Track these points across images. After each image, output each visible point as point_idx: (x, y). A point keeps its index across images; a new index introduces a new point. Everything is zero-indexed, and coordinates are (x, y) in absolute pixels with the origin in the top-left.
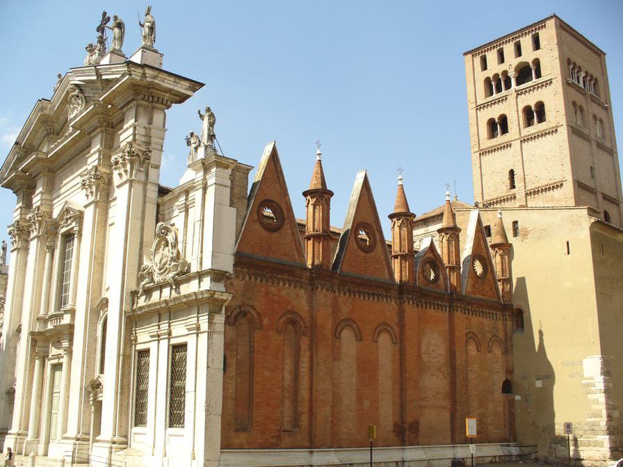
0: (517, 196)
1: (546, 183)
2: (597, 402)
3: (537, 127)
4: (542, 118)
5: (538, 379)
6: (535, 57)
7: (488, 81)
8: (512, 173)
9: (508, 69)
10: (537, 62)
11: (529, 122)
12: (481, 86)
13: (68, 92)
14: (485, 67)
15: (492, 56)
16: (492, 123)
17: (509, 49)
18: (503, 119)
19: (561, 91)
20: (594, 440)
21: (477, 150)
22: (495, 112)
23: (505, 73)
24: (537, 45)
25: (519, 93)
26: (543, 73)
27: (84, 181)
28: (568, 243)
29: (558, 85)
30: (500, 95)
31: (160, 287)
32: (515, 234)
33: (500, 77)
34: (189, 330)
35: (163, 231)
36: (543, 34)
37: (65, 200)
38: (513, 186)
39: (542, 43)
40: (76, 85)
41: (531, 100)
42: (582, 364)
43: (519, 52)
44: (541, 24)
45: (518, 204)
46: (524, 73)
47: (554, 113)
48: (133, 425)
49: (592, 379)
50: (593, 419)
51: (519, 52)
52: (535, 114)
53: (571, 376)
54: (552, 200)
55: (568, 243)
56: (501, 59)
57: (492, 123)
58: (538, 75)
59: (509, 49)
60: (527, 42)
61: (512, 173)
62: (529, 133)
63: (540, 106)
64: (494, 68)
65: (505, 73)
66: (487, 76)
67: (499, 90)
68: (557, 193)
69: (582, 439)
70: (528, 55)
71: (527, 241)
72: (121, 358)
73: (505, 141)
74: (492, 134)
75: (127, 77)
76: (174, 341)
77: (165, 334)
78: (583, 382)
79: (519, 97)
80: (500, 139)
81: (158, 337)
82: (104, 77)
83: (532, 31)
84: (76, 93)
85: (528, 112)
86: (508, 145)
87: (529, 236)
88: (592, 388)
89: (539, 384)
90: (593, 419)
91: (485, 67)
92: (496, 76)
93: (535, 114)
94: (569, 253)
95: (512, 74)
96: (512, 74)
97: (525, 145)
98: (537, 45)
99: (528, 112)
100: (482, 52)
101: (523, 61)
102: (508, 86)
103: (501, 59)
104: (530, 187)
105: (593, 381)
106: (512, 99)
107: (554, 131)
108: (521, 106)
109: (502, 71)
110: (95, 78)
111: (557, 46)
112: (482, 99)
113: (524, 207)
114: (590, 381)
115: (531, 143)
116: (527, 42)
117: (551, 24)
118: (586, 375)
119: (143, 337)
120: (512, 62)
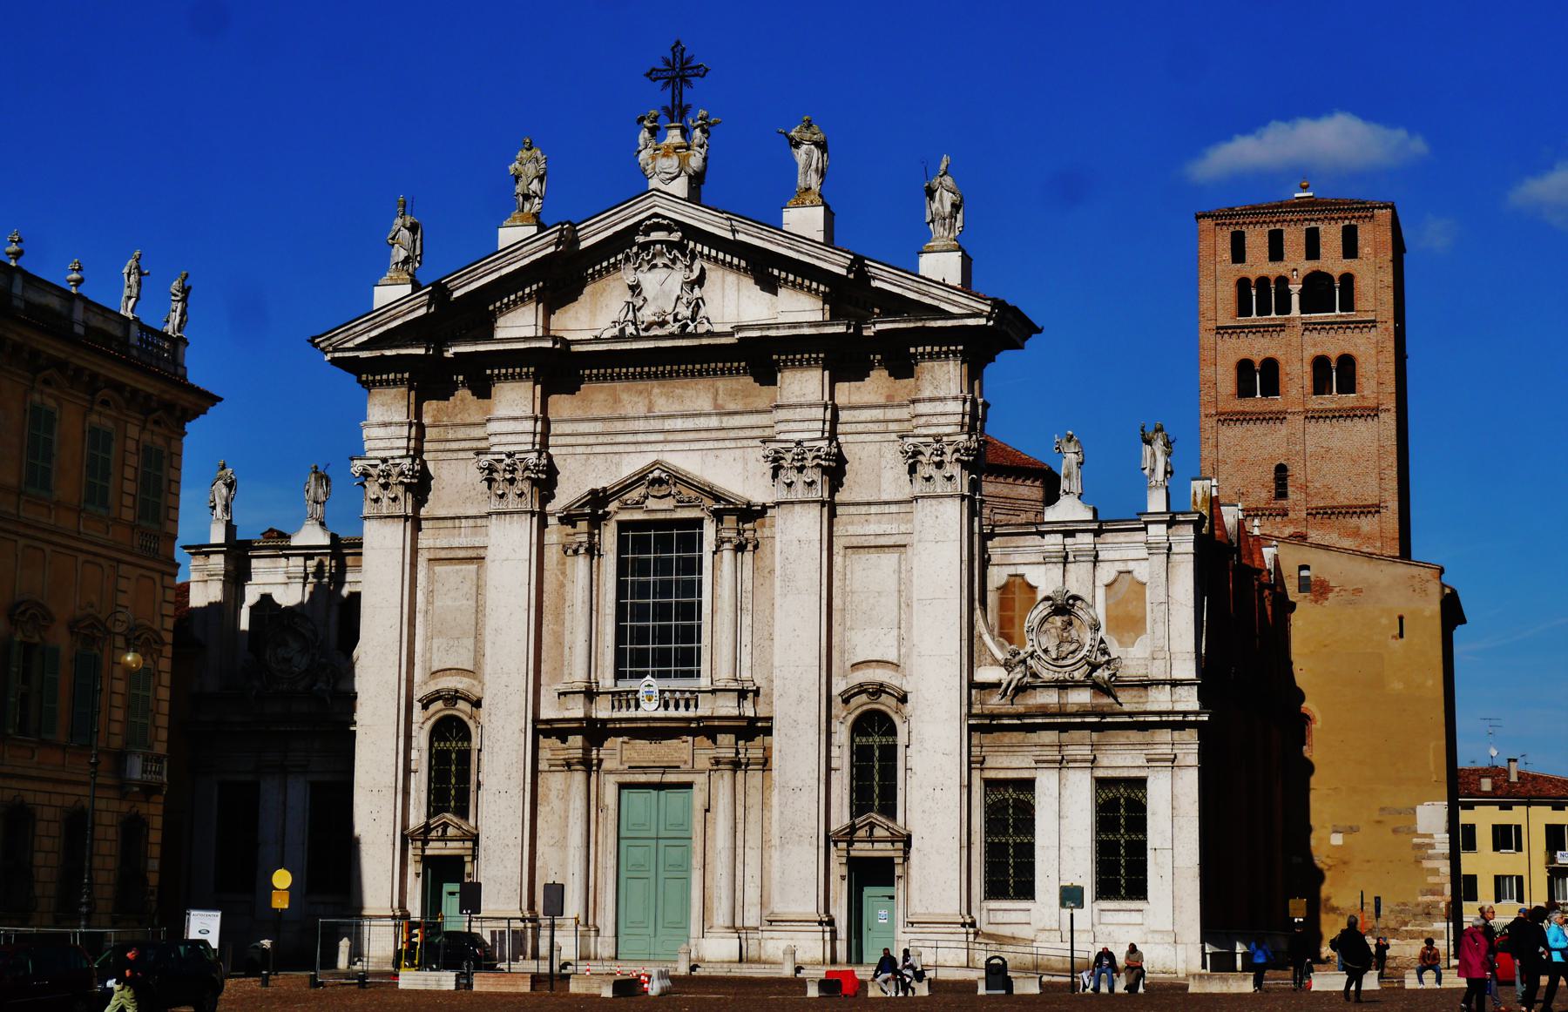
0: (1291, 514)
1: (1346, 503)
2: (1436, 872)
3: (1333, 400)
4: (1348, 385)
5: (1336, 832)
6: (1346, 270)
7: (1243, 285)
8: (1281, 471)
9: (1290, 277)
10: (1348, 279)
11: (1320, 387)
12: (1228, 293)
13: (634, 229)
14: (1238, 254)
15: (1257, 240)
16: (1244, 367)
17: (1294, 238)
18: (1271, 366)
19: (1393, 351)
20: (1429, 929)
21: (1214, 412)
22: (1257, 348)
23: (1283, 281)
24: (1350, 248)
25: (1308, 327)
26: (1359, 305)
27: (776, 452)
28: (1401, 618)
29: (1384, 335)
30: (1264, 320)
31: (1062, 686)
32: (1305, 584)
33: (1273, 286)
34: (1148, 761)
35: (1071, 602)
36: (1365, 234)
37: (649, 459)
38: (1281, 493)
39: (1365, 249)
40: (682, 226)
41: (1333, 346)
42: (1415, 812)
43: (1313, 251)
44: (1365, 209)
45: (1288, 531)
46: (1319, 292)
47: (1373, 383)
48: (983, 899)
49: (1431, 836)
50: (1429, 898)
51: (1313, 251)
52: (1334, 374)
53: (1395, 831)
54: (1356, 533)
55: (1401, 618)
56: (1276, 253)
57: (1244, 367)
58: (1348, 305)
59: (1294, 238)
60: (1331, 235)
61: (1281, 471)
62: (1321, 407)
63: (1347, 362)
64: (1258, 264)
65: (1283, 281)
66: (1243, 274)
67: (1264, 310)
68: (1367, 524)
69: (1409, 928)
70: (1332, 262)
71: (1326, 603)
72: (966, 790)
73: (1275, 408)
74: (1245, 390)
75: (983, 321)
76: (1100, 773)
77: (1085, 761)
78: (1415, 840)
79: (1307, 333)
80: (1257, 403)
81: (1061, 764)
82: (875, 284)
83: (1346, 218)
84: (676, 237)
85: (1320, 364)
86: (1279, 417)
87: (1331, 595)
88: (1430, 851)
89: (1337, 839)
90: (1429, 898)
91: (1238, 254)
92: (1263, 282)
93: (1334, 374)
94: (1401, 635)
95: (1295, 288)
96: (1295, 288)
97: (1312, 427)
98: (1350, 248)
99: (1320, 364)
100: (1237, 223)
101: (1325, 270)
102: (1284, 308)
103: (1276, 253)
104: (1317, 502)
105: (1433, 841)
106: (1293, 336)
107: (1373, 412)
108: (1311, 352)
109: (1277, 275)
110: (843, 272)
111: (1391, 264)
112: (1227, 317)
113: (1301, 538)
114: (1427, 841)
115: (1324, 426)
116: (1331, 235)
117: (1384, 215)
118: (1420, 830)
119: (1009, 762)
120: (1296, 266)
